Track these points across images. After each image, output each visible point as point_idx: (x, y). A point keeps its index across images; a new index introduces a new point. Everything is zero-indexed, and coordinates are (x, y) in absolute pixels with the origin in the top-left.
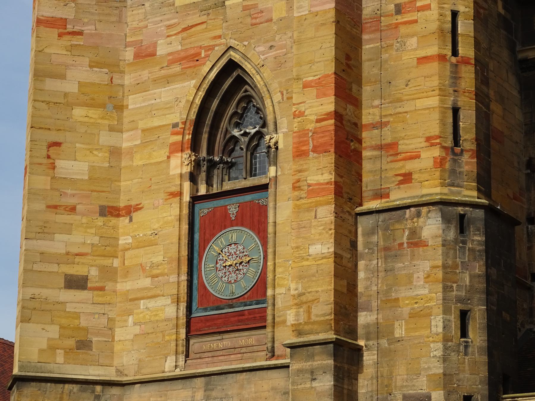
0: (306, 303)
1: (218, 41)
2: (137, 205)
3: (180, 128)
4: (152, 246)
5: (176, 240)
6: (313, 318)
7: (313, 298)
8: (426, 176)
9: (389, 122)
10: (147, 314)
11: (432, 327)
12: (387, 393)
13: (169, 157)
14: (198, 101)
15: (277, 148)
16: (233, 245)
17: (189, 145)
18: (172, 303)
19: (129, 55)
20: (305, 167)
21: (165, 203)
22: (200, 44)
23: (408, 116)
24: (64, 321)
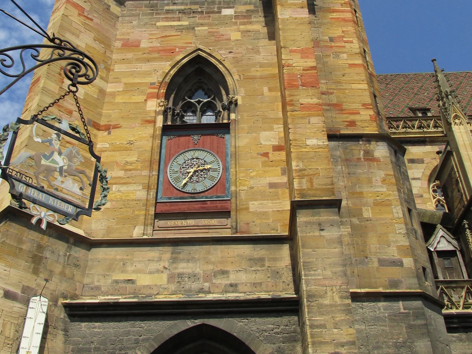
0: (308, 175)
1: (189, 45)
3: (157, 86)
4: (127, 150)
5: (149, 148)
6: (315, 186)
7: (314, 173)
8: (366, 124)
9: (333, 92)
10: (118, 195)
11: (394, 213)
12: (363, 256)
13: (146, 100)
14: (172, 73)
15: (236, 104)
16: (195, 160)
17: (164, 96)
18: (143, 189)
19: (118, 44)
20: (296, 93)
21: (141, 126)
22: (176, 45)
23: (347, 91)
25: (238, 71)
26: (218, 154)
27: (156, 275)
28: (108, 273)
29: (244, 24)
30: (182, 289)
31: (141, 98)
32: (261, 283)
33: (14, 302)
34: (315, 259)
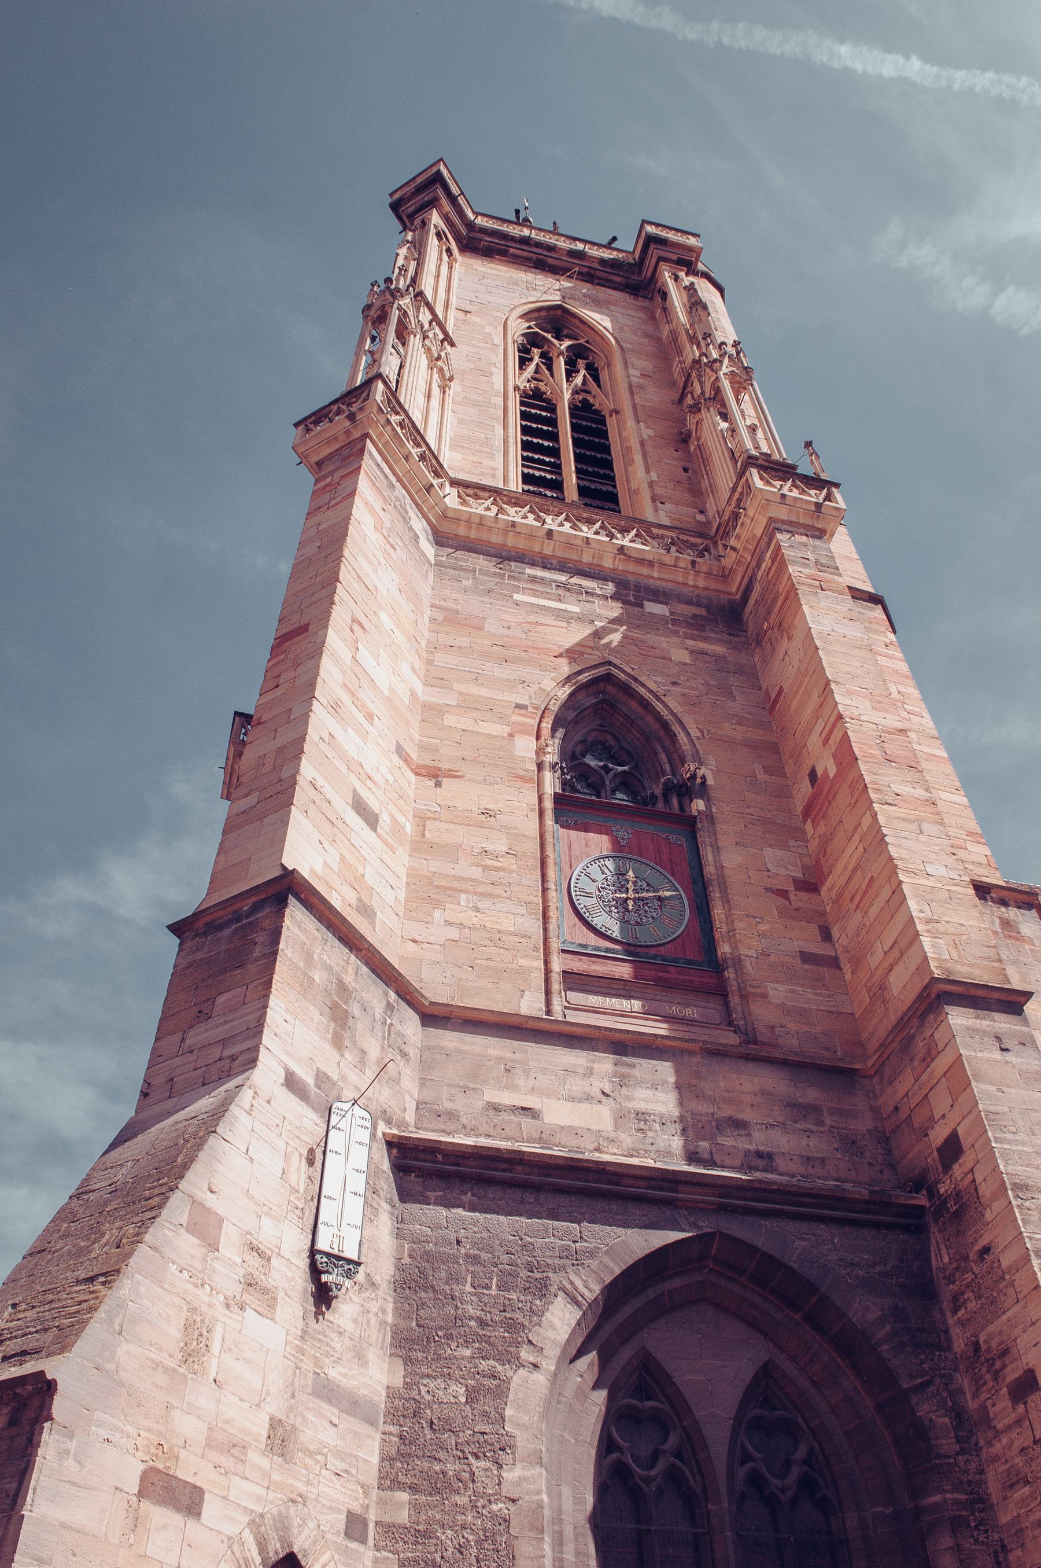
2: (452, 771)
24: (346, 853)
25: (696, 721)
26: (673, 874)
27: (585, 1106)
28: (471, 1085)
29: (693, 638)
30: (650, 1148)
31: (500, 730)
32: (823, 1160)
33: (302, 1103)
34: (1006, 1109)
